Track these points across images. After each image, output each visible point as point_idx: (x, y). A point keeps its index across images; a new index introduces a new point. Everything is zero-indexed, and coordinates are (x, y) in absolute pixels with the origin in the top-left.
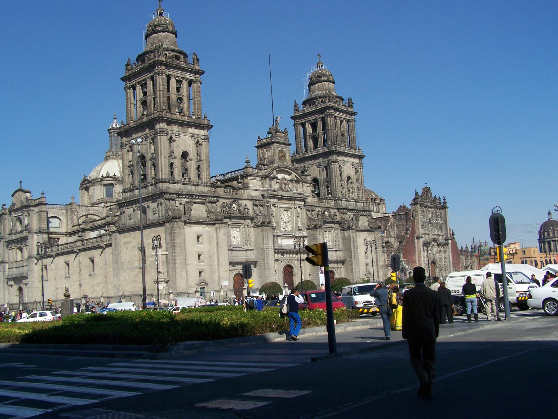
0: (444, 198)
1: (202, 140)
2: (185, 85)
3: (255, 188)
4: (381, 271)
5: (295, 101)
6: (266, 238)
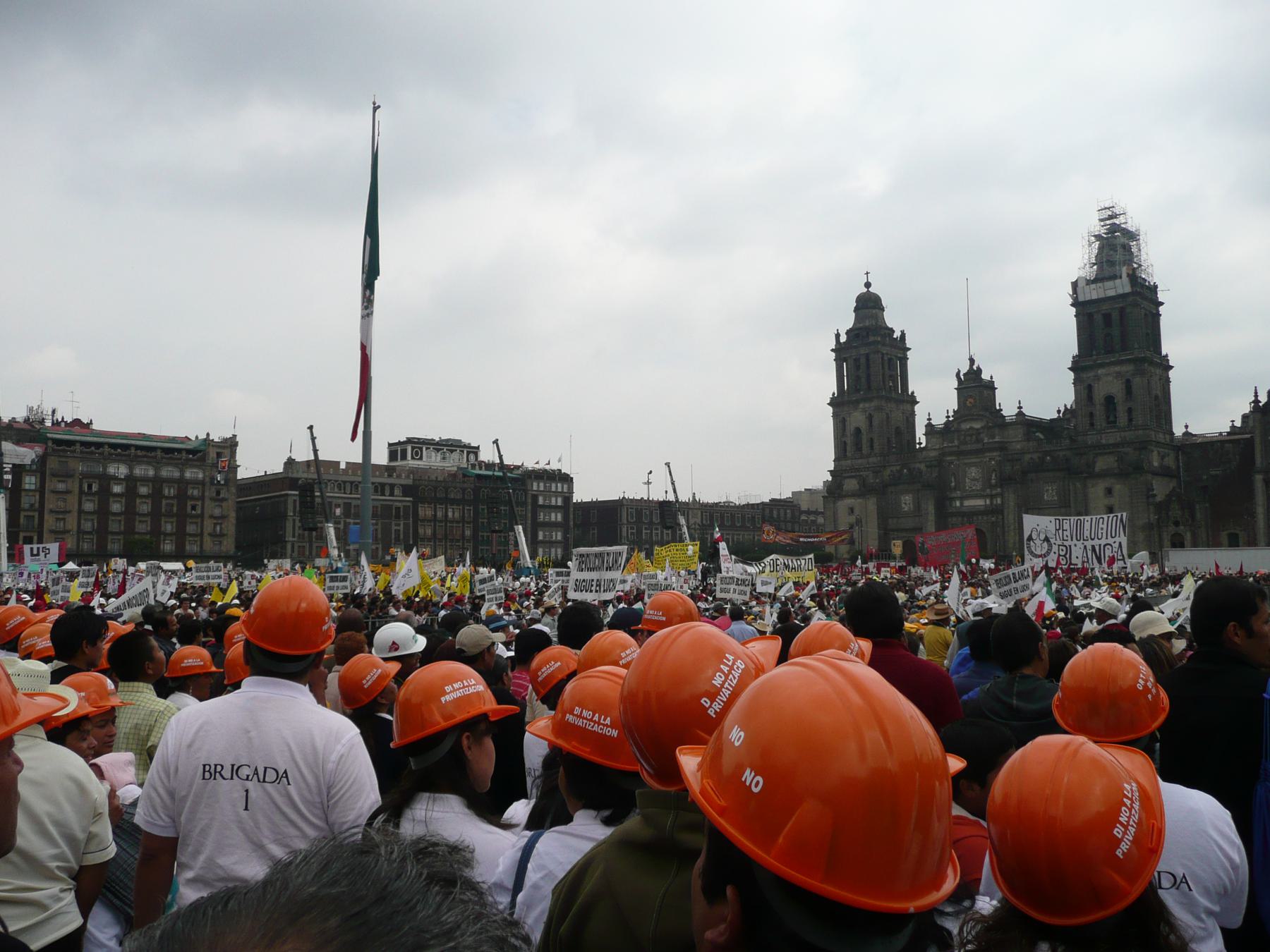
2: (863, 361)
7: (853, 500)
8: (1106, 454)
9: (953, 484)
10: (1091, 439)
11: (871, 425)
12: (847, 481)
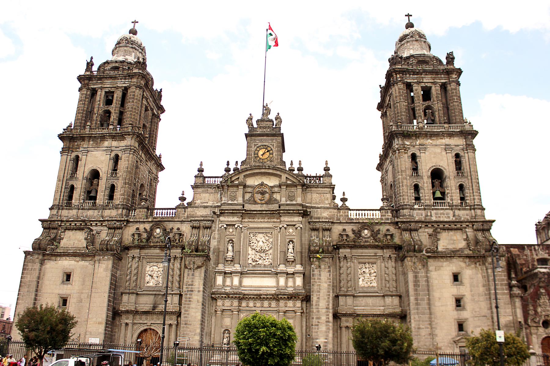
1: (123, 152)
2: (118, 95)
3: (206, 204)
5: (380, 86)
6: (188, 275)
7: (73, 262)
9: (230, 254)
10: (418, 215)
11: (115, 169)
12: (69, 233)
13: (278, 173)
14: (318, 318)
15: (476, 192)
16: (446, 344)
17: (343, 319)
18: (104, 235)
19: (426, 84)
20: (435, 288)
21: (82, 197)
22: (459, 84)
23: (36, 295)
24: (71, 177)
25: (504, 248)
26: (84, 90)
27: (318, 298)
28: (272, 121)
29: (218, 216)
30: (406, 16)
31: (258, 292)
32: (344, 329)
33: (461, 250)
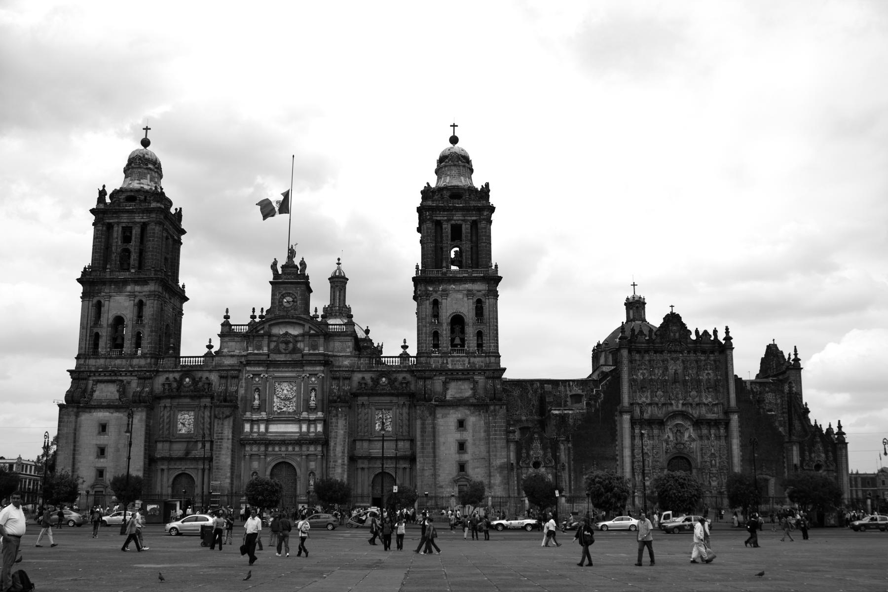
0: (727, 329)
2: (136, 231)
3: (232, 353)
4: (498, 475)
6: (218, 424)
7: (107, 414)
8: (460, 379)
9: (257, 402)
11: (140, 316)
13: (302, 322)
14: (335, 461)
15: (492, 340)
16: (447, 483)
17: (360, 461)
18: (134, 385)
19: (456, 222)
20: (440, 433)
21: (109, 345)
22: (491, 222)
23: (75, 446)
24: (94, 324)
25: (538, 384)
26: (99, 225)
27: (335, 444)
28: (296, 267)
29: (245, 365)
30: (451, 126)
31: (283, 438)
32: (360, 471)
33: (468, 398)
